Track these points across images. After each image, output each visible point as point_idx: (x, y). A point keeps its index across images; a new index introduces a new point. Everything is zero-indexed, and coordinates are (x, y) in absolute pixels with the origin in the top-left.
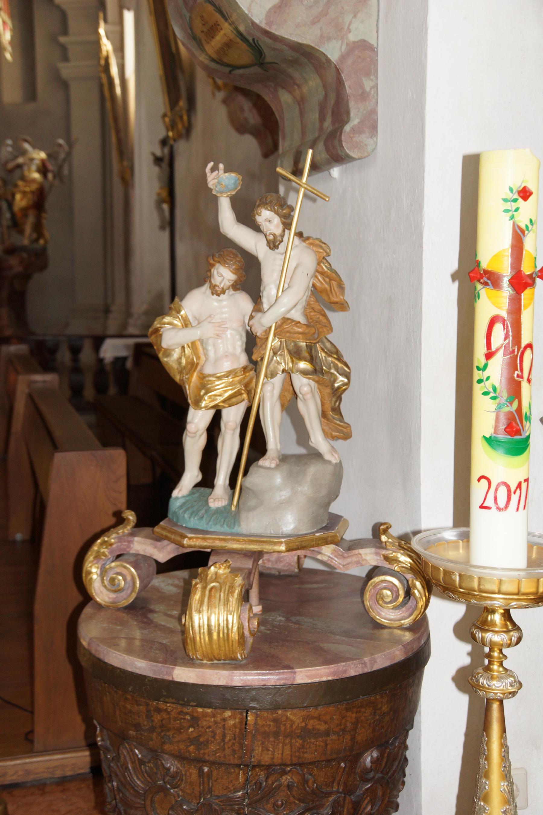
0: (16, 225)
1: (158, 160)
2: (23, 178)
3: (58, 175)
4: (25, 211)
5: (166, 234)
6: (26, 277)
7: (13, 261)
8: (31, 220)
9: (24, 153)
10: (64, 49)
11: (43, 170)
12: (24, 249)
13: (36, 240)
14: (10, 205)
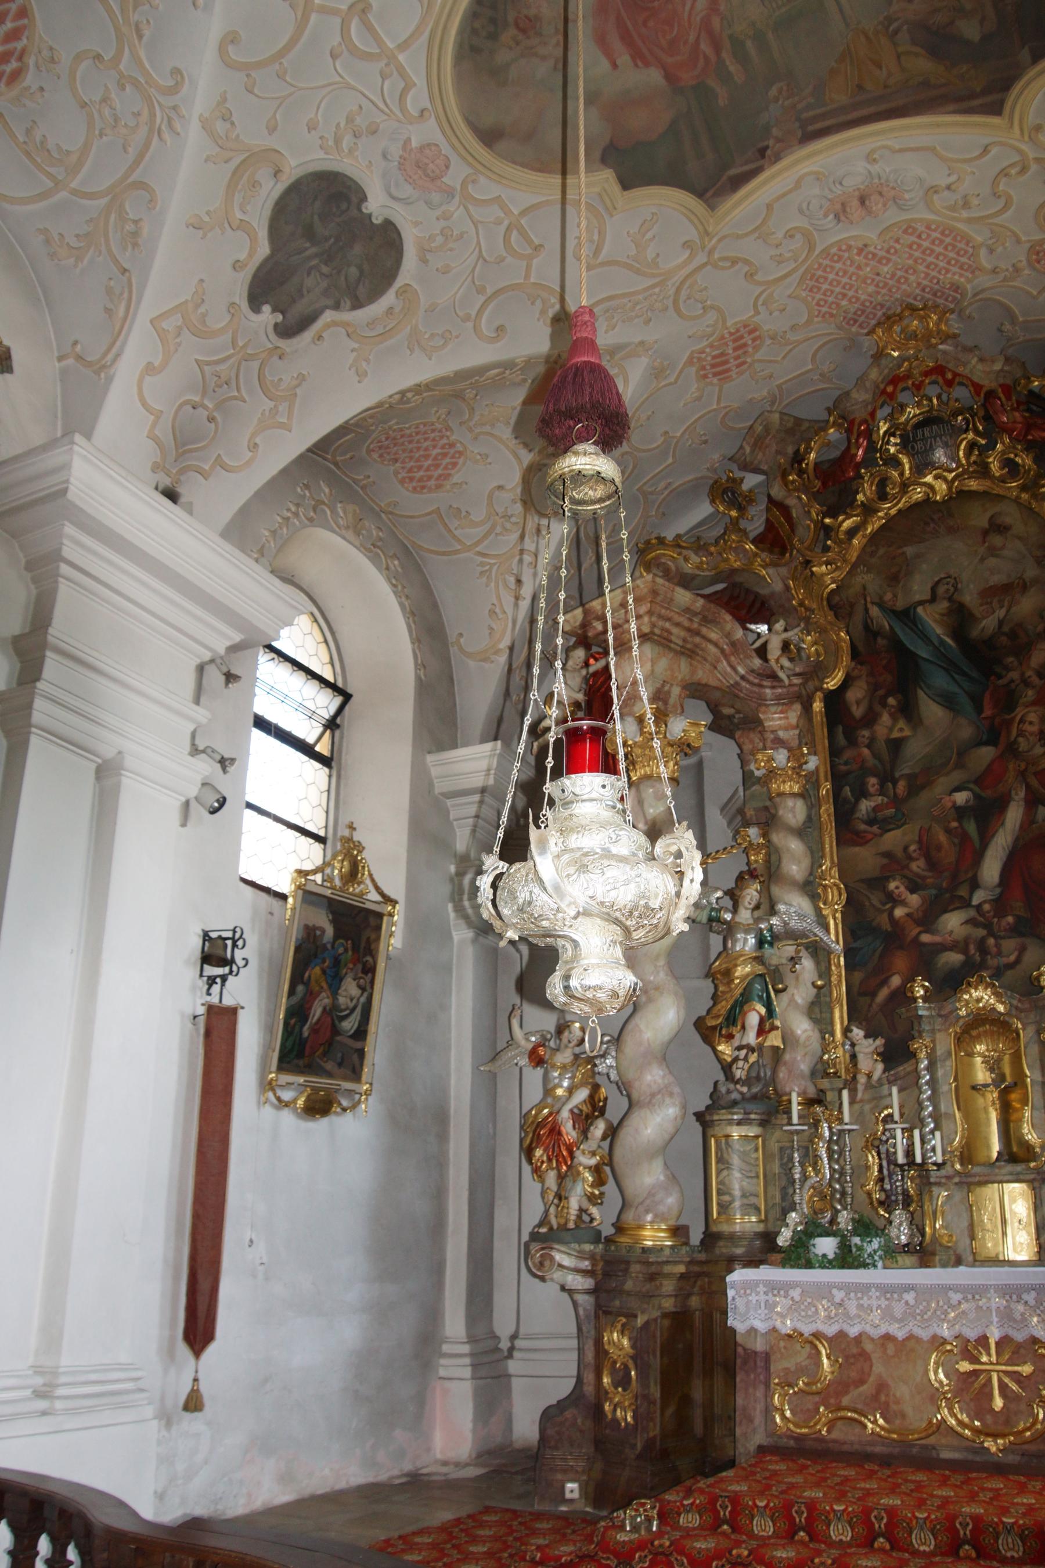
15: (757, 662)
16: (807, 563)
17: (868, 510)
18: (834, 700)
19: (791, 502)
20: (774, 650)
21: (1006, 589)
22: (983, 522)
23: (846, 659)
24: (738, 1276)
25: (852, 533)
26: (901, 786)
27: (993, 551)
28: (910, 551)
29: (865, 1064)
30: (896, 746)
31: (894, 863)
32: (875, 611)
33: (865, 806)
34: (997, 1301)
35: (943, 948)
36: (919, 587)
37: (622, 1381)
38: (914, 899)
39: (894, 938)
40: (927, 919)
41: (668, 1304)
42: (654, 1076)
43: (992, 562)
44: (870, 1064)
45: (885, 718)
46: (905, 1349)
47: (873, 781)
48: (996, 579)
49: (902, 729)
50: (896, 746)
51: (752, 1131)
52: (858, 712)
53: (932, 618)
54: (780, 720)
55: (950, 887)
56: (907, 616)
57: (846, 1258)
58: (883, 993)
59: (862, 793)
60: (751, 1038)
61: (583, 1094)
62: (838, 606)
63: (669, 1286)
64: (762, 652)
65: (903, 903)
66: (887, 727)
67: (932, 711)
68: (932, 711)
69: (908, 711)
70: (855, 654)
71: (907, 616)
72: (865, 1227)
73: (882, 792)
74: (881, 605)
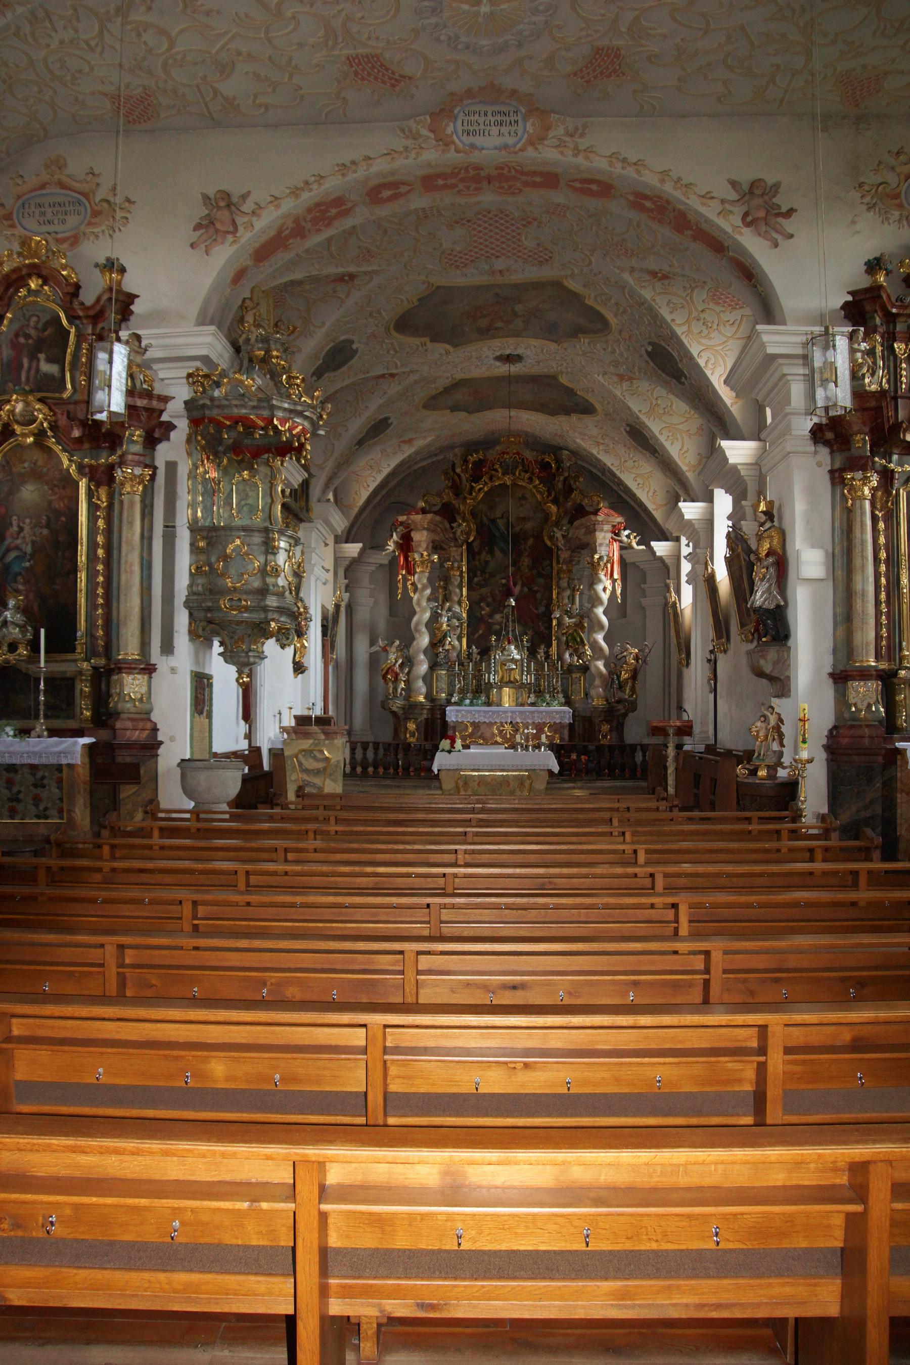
0: (621, 687)
1: (709, 661)
2: (626, 663)
3: (645, 662)
4: (627, 679)
5: (712, 696)
6: (625, 715)
7: (620, 707)
8: (630, 684)
9: (627, 650)
10: (643, 590)
11: (637, 658)
12: (626, 700)
13: (632, 695)
14: (619, 677)
15: (451, 535)
16: (465, 498)
17: (486, 484)
18: (470, 546)
19: (462, 475)
20: (459, 533)
21: (524, 519)
22: (520, 496)
23: (474, 533)
24: (448, 708)
25: (480, 489)
26: (487, 576)
27: (522, 505)
28: (497, 499)
29: (475, 656)
30: (487, 562)
31: (483, 599)
32: (484, 518)
33: (476, 579)
34: (510, 714)
35: (494, 624)
36: (498, 513)
37: (413, 735)
38: (488, 609)
39: (481, 619)
40: (491, 615)
41: (425, 716)
42: (422, 657)
43: (521, 509)
44: (476, 657)
45: (484, 553)
46: (491, 724)
47: (479, 573)
48: (521, 515)
49: (489, 558)
50: (487, 562)
51: (444, 672)
52: (476, 550)
53: (501, 523)
54: (454, 552)
55: (500, 606)
56: (493, 521)
57: (472, 704)
58: (477, 635)
59: (476, 576)
60: (447, 647)
61: (400, 661)
62: (474, 514)
63: (425, 712)
64: (454, 533)
65: (484, 609)
66: (484, 556)
67: (498, 553)
68: (498, 553)
69: (491, 552)
70: (477, 531)
71: (493, 521)
72: (474, 698)
73: (481, 575)
74: (486, 516)
